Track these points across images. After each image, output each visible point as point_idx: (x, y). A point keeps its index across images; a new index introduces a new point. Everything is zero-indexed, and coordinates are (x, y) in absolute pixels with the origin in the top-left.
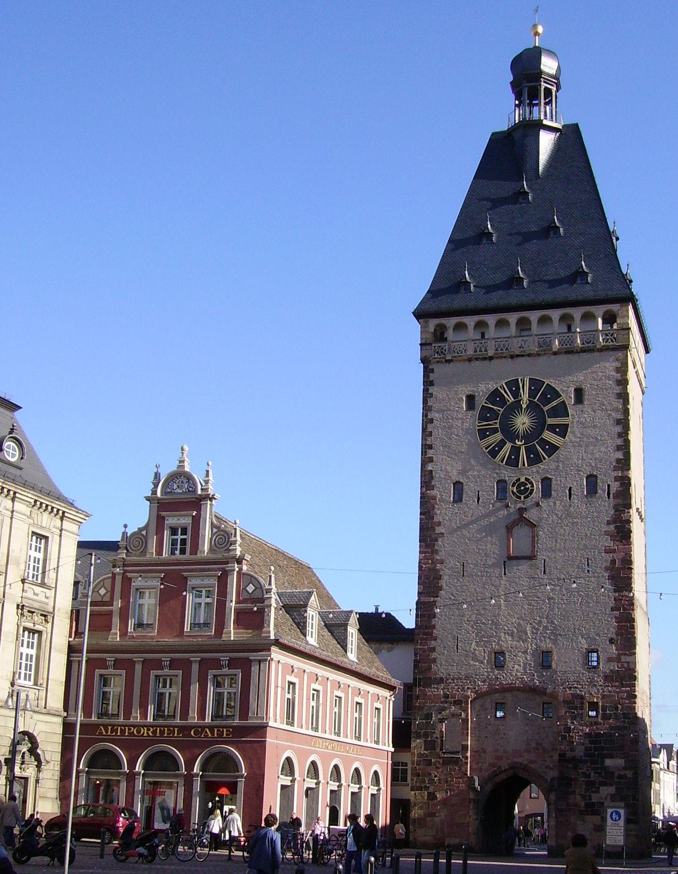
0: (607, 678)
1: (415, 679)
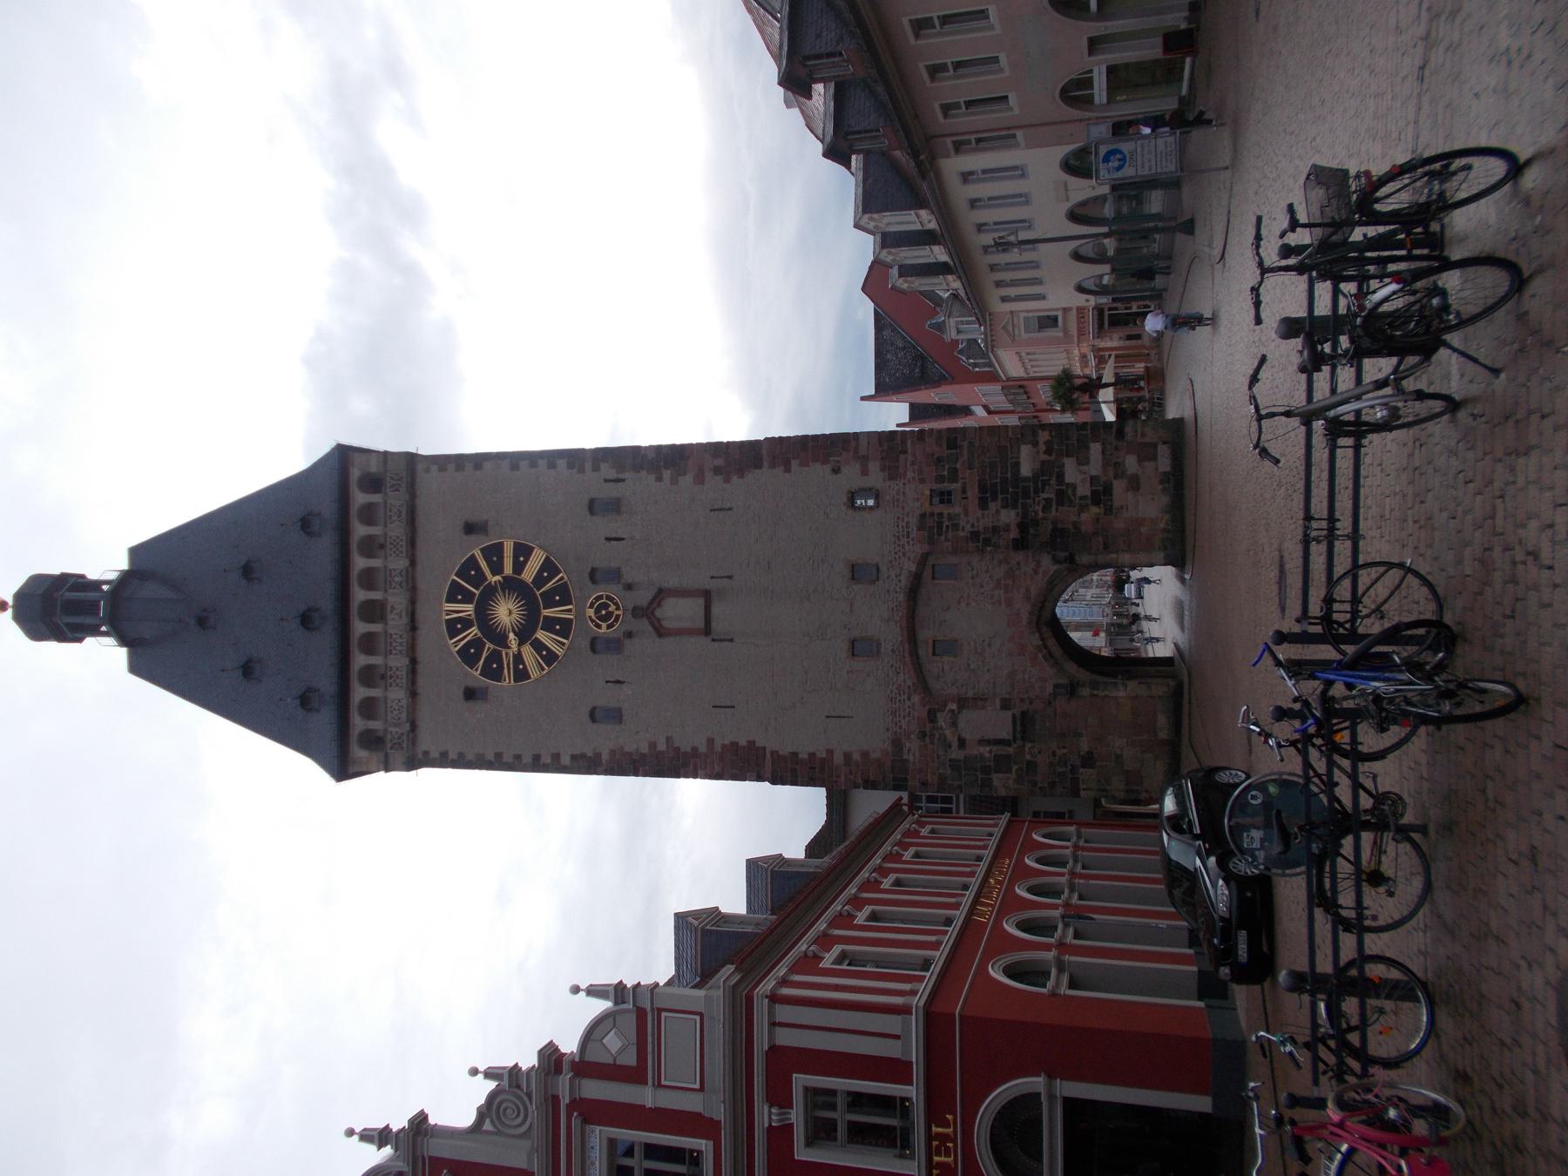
0: (893, 473)
1: (896, 788)
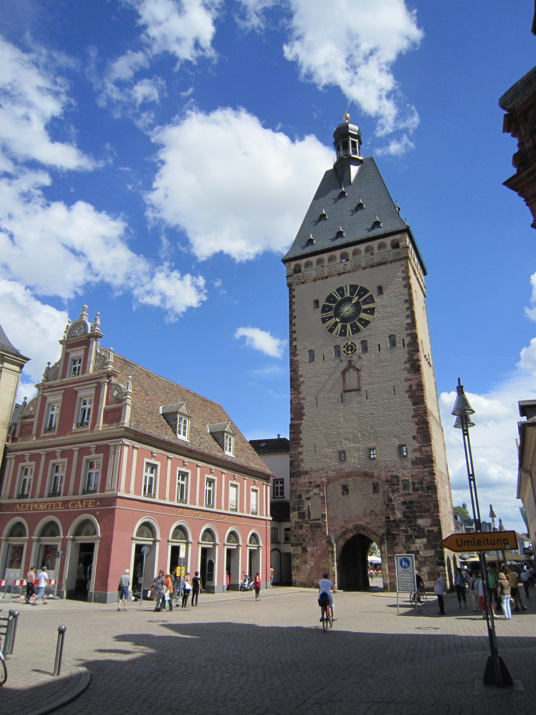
0: (415, 463)
